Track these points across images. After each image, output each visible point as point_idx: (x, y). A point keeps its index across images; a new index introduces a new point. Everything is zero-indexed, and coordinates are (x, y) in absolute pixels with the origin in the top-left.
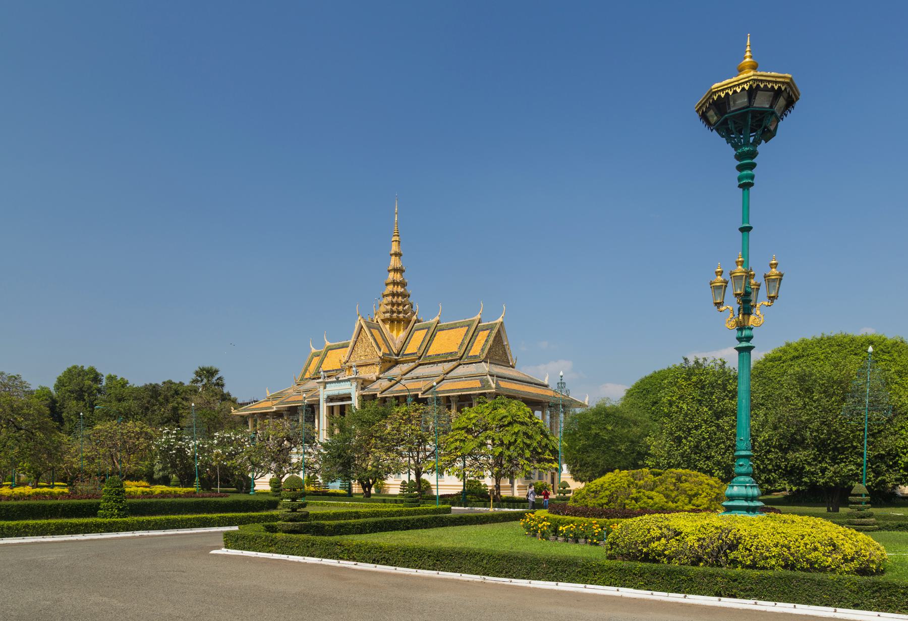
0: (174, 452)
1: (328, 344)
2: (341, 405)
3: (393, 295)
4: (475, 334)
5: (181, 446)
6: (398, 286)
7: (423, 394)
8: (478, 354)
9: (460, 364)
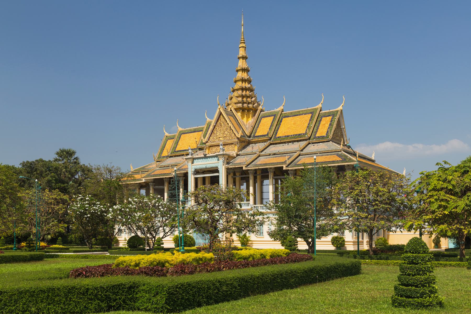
0: (89, 215)
1: (180, 129)
2: (211, 177)
3: (242, 89)
4: (319, 119)
5: (94, 210)
6: (245, 83)
8: (325, 135)
9: (309, 143)
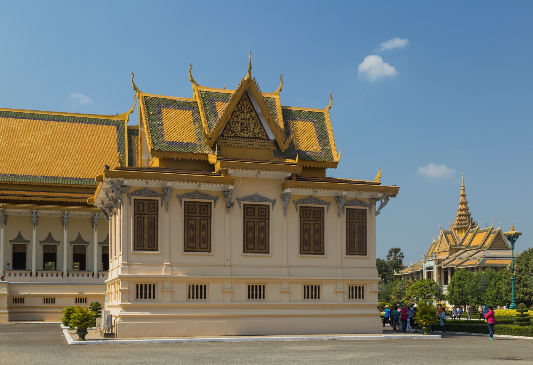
3: (460, 216)
7: (457, 266)
